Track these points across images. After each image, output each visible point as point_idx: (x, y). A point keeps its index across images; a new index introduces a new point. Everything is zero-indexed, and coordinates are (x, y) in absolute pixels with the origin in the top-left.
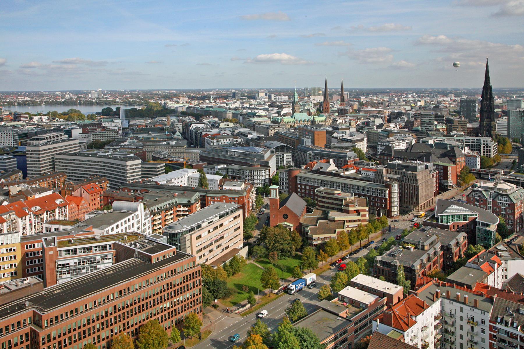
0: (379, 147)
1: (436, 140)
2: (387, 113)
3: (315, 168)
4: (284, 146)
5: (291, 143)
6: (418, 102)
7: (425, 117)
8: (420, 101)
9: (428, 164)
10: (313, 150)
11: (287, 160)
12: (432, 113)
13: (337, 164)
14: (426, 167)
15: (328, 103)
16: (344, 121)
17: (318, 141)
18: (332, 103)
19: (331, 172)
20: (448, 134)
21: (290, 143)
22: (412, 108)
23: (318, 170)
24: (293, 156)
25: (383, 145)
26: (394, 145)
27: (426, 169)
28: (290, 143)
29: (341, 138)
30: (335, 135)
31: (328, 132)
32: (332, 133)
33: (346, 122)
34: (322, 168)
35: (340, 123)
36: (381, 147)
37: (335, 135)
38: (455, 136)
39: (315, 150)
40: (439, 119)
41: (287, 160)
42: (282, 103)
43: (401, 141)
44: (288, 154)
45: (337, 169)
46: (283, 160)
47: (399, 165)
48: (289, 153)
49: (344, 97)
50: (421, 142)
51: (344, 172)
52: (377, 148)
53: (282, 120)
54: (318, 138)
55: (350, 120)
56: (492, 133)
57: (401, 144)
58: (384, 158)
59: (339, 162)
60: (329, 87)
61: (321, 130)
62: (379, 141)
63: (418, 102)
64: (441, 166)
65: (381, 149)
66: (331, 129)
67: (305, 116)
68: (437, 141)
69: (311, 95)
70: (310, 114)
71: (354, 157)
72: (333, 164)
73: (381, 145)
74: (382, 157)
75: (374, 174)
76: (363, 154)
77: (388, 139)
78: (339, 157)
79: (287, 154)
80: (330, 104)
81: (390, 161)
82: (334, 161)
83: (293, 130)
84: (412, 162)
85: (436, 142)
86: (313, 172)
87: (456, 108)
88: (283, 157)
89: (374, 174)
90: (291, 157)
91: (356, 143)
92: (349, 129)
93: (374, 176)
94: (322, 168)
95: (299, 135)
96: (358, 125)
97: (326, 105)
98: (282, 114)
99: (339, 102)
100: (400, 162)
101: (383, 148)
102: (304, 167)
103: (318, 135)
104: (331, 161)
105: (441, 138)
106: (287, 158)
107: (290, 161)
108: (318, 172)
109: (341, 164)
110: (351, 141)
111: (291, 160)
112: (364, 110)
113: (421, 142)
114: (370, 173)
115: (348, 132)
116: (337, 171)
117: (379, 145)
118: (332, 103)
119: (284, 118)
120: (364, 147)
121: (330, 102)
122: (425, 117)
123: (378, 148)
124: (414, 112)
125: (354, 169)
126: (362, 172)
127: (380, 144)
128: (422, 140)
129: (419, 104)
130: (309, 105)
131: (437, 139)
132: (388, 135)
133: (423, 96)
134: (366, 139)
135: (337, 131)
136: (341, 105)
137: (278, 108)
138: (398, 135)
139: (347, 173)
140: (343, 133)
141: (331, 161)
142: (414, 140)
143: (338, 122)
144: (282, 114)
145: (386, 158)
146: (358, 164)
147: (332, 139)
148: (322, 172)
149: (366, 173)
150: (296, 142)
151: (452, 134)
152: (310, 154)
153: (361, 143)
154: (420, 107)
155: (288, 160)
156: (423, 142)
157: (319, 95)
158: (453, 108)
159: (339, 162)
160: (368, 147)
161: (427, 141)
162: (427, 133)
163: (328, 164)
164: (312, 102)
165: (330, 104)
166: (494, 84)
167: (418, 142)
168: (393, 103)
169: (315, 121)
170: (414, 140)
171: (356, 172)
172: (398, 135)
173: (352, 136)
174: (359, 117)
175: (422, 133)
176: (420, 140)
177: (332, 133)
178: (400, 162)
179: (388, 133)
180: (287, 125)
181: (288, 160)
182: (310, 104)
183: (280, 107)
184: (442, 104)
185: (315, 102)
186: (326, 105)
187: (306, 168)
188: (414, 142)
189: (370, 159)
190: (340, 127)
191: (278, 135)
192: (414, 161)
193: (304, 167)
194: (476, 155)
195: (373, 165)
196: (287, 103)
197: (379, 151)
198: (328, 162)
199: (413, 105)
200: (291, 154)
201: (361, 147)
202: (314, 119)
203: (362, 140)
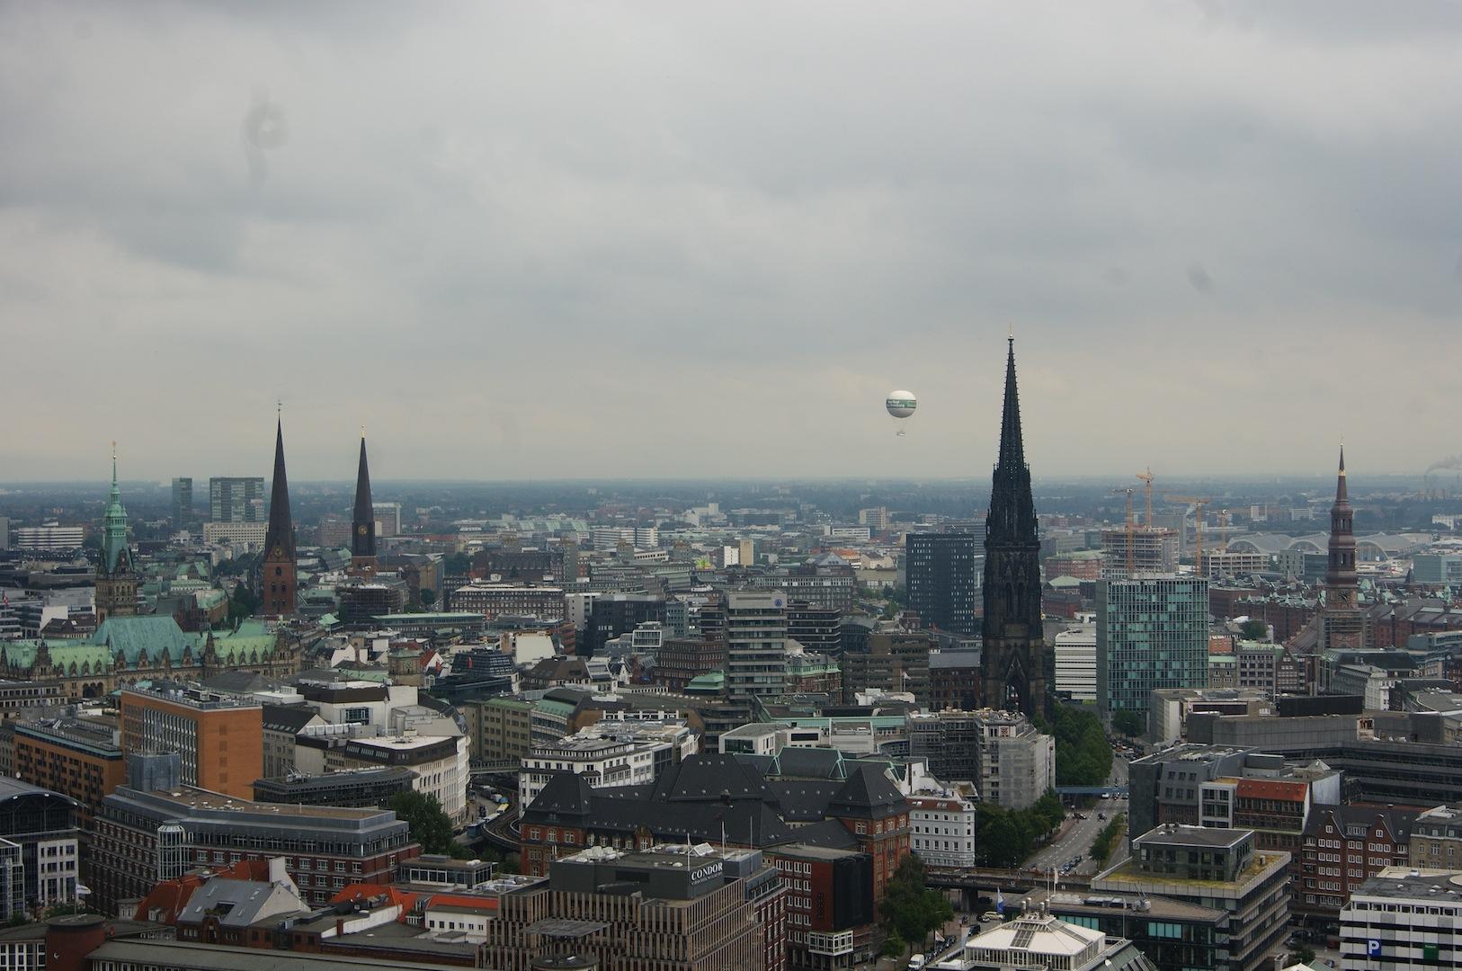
0: (526, 782)
1: (789, 733)
2: (578, 602)
3: (193, 911)
4: (40, 797)
5: (82, 781)
6: (727, 549)
7: (746, 623)
8: (736, 545)
9: (739, 856)
10: (186, 811)
11: (52, 875)
12: (778, 603)
13: (312, 880)
14: (731, 868)
15: (291, 556)
16: (364, 654)
17: (223, 762)
18: (311, 562)
19: (273, 924)
20: (844, 708)
21: (75, 784)
22: (694, 581)
23: (209, 918)
24: (84, 853)
25: (548, 770)
26: (599, 767)
27: (727, 881)
28: (75, 784)
29: (342, 743)
30: (313, 727)
31: (273, 713)
32: (298, 716)
33: (373, 656)
34: (225, 909)
35: (345, 664)
36: (534, 779)
37: (313, 727)
38: (876, 711)
39: (198, 814)
40: (807, 625)
41: (52, 875)
42: (48, 566)
43: (631, 747)
44: (58, 844)
45: (303, 907)
46: (31, 877)
47: (599, 867)
48: (68, 836)
49: (371, 527)
50: (722, 750)
51: (339, 926)
52: (516, 786)
53: (43, 656)
54: (223, 746)
55: (394, 648)
56: (1032, 691)
57: (630, 760)
58: (544, 836)
59: (323, 869)
60: (292, 476)
61: (237, 707)
62: (527, 751)
63: (727, 549)
64: (803, 860)
65: (534, 792)
66: (289, 696)
67: (160, 633)
68: (795, 737)
69: (210, 520)
70: (191, 618)
71: (395, 838)
72: (290, 882)
73: (535, 773)
74: (535, 833)
75: (483, 920)
76: (444, 822)
77: (569, 739)
78: (322, 846)
79: (51, 844)
80: (300, 562)
81: (566, 848)
82: (294, 864)
83: (98, 712)
84: (671, 852)
85: (790, 743)
86: (182, 931)
87: (894, 576)
88: (31, 862)
89: (483, 920)
90: (75, 857)
91: (416, 769)
92: (380, 694)
93: (485, 932)
94: (225, 909)
95: (126, 738)
96: (435, 671)
97: (279, 572)
98: (43, 624)
99: (346, 554)
100: (612, 853)
101: (544, 785)
102: (134, 911)
103: (223, 730)
104: (278, 867)
105: (816, 724)
106: (52, 867)
107: (70, 881)
108: (214, 931)
109: (330, 881)
110: (391, 757)
111: (75, 873)
112: (468, 594)
113: (722, 750)
114: (468, 919)
115: (378, 709)
116: (303, 921)
117: (527, 770)
118: (311, 562)
119: (50, 643)
120: (455, 786)
121: (303, 556)
122: (746, 623)
123: (522, 786)
124: (705, 600)
125: (391, 904)
126: (430, 916)
127: (531, 764)
128: (723, 737)
129: (731, 557)
130: (192, 573)
131: (797, 730)
132: (573, 717)
133: (749, 520)
134: (463, 745)
135: (324, 706)
136: (357, 570)
137: (21, 593)
138: (621, 715)
139: (352, 926)
140: (353, 716)
141: (278, 867)
142: (691, 738)
143: (338, 657)
144: (43, 624)
145: (552, 836)
146: (415, 875)
147: (301, 751)
148: (229, 929)
149: (447, 918)
150: (105, 776)
151: (862, 700)
152: (174, 837)
153: (442, 767)
154: (734, 575)
155: (57, 875)
156: (729, 745)
157: (250, 516)
158: (880, 575)
159: (323, 869)
160: (474, 788)
161: (750, 744)
162: (754, 705)
163: (257, 888)
164: (208, 556)
165: (300, 562)
166: (1042, 463)
167: (707, 744)
168: (613, 554)
169: (218, 661)
170: (691, 738)
171: (401, 921)
172: (621, 715)
173: (396, 731)
174: (440, 632)
175: (733, 702)
176: (716, 740)
177: (298, 716)
178: (612, 853)
179: (570, 709)
180: (68, 685)
181: (57, 875)
182: (201, 568)
183: (37, 587)
184: (832, 557)
185: (229, 555)
186: (279, 572)
187: (142, 916)
188: (690, 746)
189: (477, 850)
190: (340, 686)
191: (12, 741)
192: (675, 847)
193: (128, 913)
194: (957, 798)
195: (483, 876)
196: (78, 564)
197: (527, 800)
198: (263, 875)
199: (703, 563)
200: (74, 842)
201: (442, 785)
202: (210, 648)
203: (446, 750)
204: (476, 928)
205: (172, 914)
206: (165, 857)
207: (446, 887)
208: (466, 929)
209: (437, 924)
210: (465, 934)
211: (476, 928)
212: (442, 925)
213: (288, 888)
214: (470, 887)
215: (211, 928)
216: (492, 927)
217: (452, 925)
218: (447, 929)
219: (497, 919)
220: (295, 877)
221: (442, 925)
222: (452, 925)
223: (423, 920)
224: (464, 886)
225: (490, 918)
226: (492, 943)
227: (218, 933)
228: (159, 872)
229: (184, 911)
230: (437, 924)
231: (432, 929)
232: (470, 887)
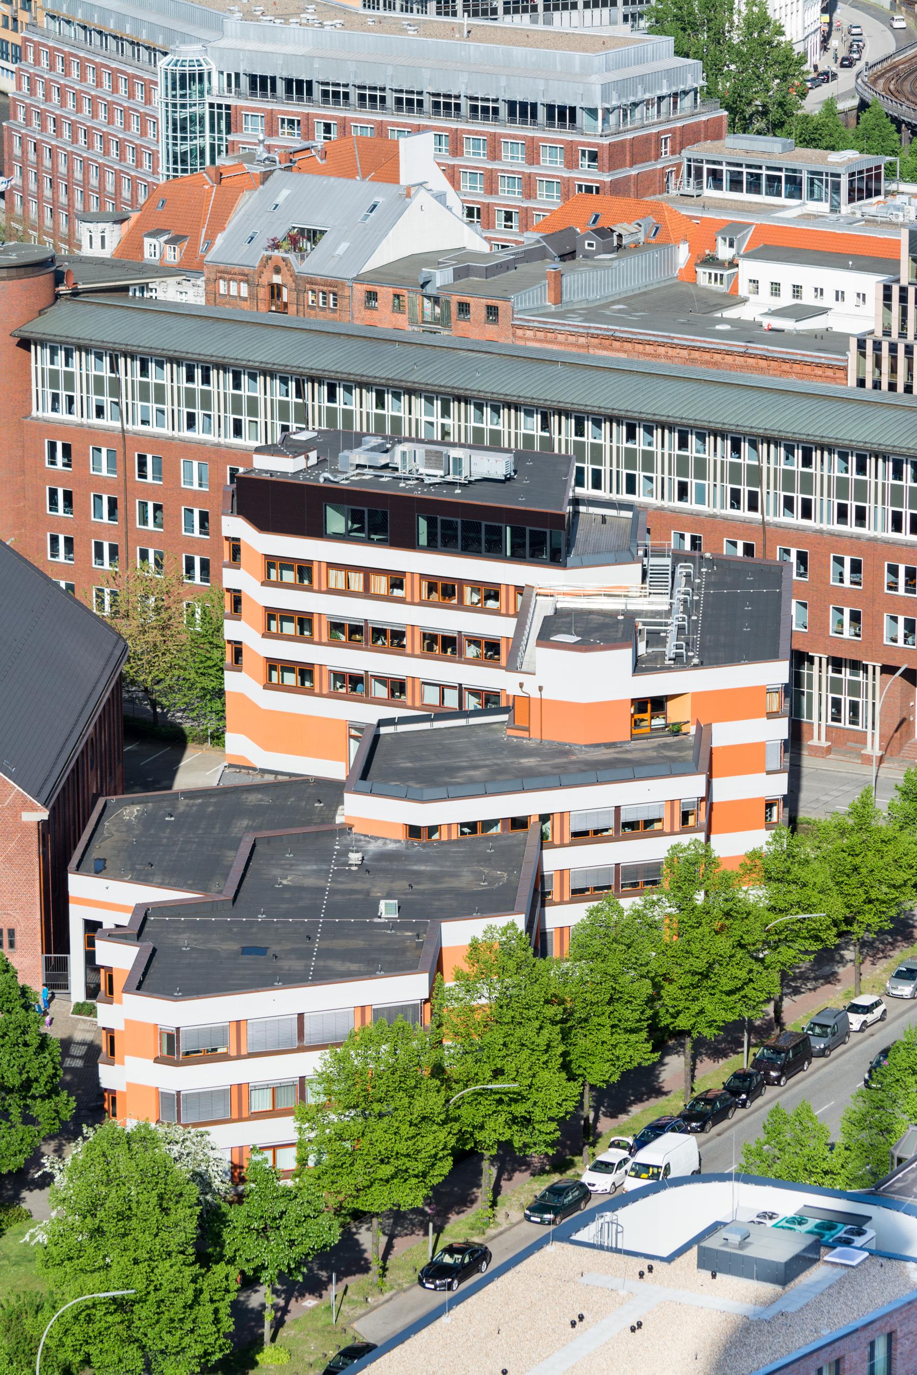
72: (441, 183)
109: (528, 186)
204: (851, 298)
205: (193, 248)
206: (175, 124)
207: (784, 207)
208: (828, 301)
209: (764, 288)
210: (823, 311)
211: (851, 298)
212: (776, 289)
213: (441, 198)
214: (835, 209)
215: (277, 279)
216: (887, 297)
217: (797, 290)
218: (786, 299)
219: (898, 281)
220: (452, 174)
221: (776, 289)
222: (797, 290)
223: (735, 278)
224: (823, 207)
225: (882, 278)
226: (887, 333)
227: (290, 290)
228: (162, 156)
229: (220, 239)
230: (764, 288)
231: (752, 297)
232: (835, 209)
